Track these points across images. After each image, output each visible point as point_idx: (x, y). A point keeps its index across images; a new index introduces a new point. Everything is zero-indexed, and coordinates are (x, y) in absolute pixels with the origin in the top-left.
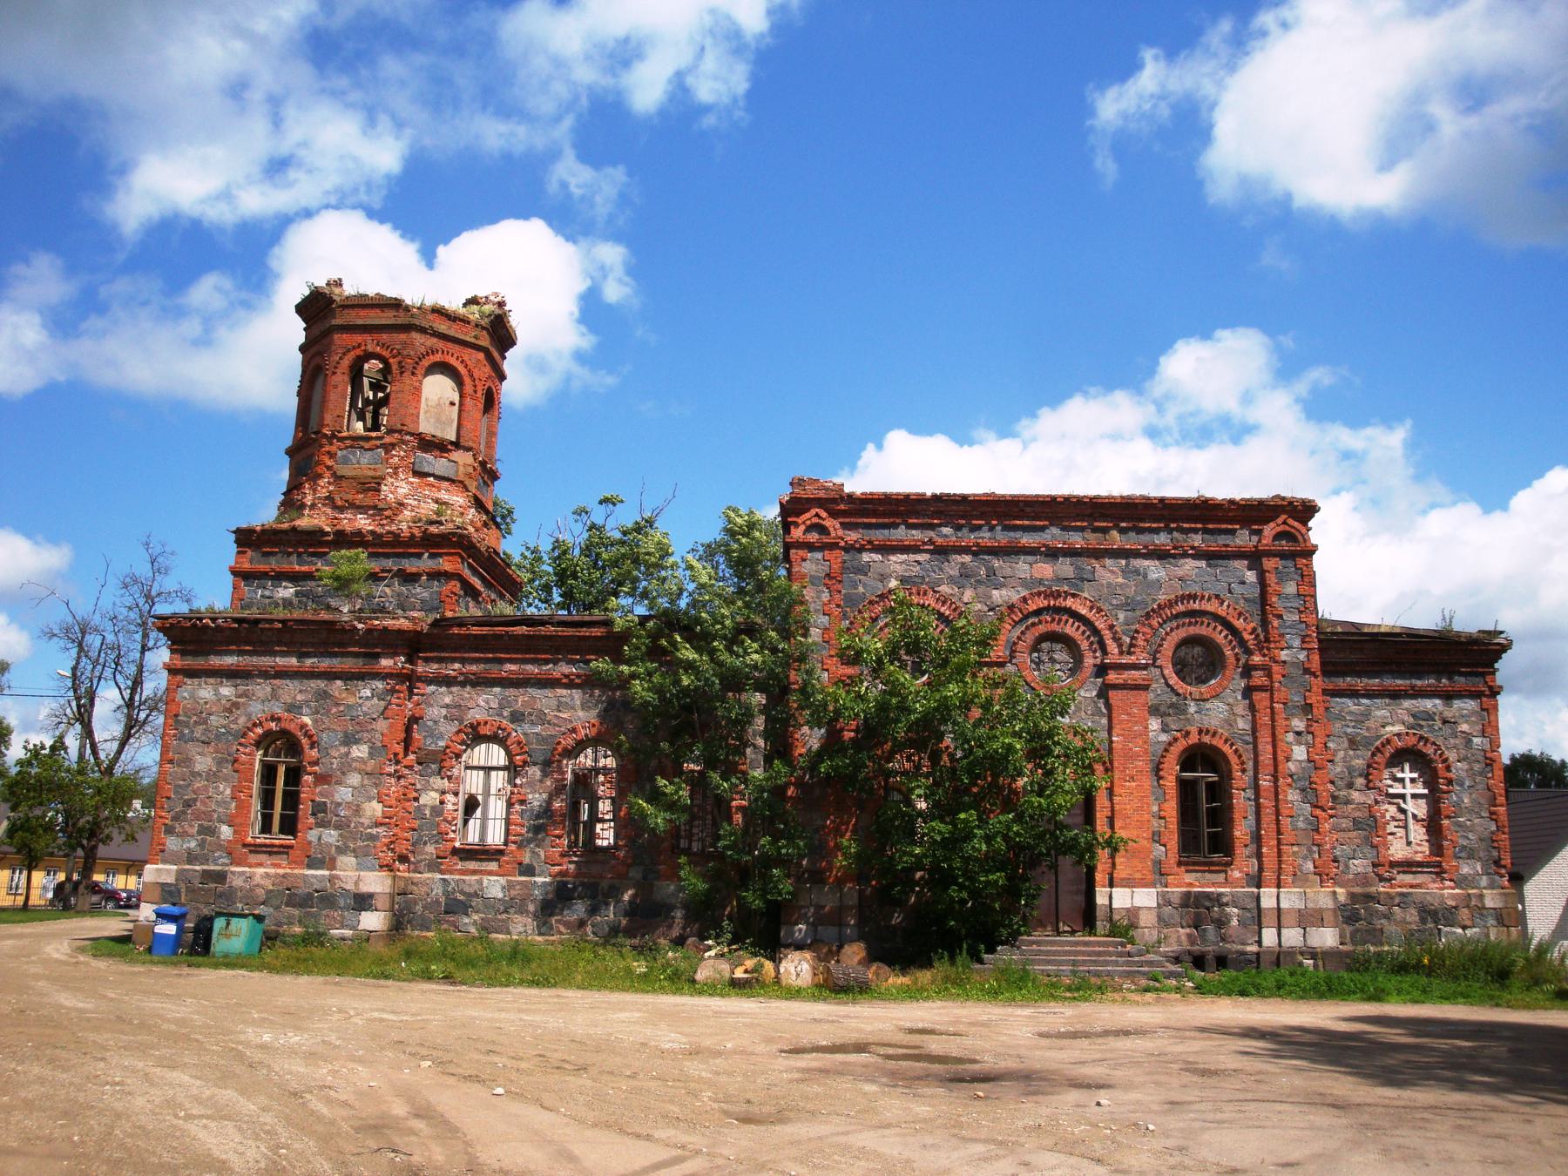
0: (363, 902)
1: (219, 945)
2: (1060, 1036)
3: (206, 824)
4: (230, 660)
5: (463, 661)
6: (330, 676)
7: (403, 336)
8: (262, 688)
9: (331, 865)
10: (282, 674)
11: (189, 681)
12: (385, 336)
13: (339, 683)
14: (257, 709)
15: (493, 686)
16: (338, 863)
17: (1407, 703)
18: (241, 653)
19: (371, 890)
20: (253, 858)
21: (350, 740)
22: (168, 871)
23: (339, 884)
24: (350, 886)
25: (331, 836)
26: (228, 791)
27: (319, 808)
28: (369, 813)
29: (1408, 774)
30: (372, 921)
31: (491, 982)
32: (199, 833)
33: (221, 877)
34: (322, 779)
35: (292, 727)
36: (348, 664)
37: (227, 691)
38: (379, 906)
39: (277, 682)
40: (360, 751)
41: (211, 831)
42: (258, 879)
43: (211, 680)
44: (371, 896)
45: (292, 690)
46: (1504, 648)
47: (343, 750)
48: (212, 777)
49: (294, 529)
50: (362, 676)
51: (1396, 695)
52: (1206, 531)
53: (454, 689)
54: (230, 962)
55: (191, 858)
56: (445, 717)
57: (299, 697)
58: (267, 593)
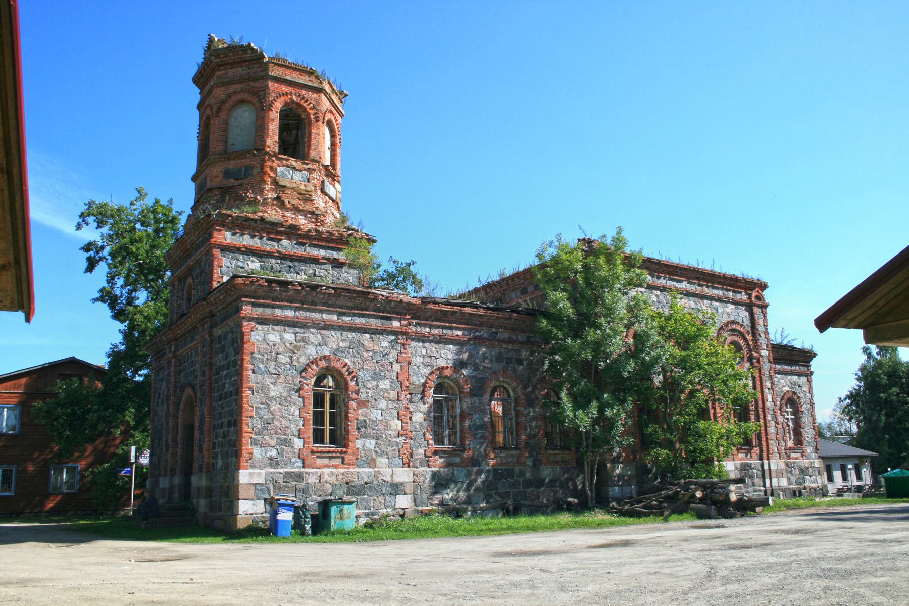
0: (396, 489)
1: (334, 524)
2: (595, 547)
3: (282, 437)
4: (290, 313)
5: (431, 327)
6: (363, 330)
7: (315, 96)
8: (314, 336)
9: (372, 463)
10: (328, 326)
11: (259, 327)
12: (304, 92)
13: (367, 336)
14: (312, 351)
15: (448, 344)
16: (377, 463)
17: (789, 377)
18: (296, 309)
19: (402, 481)
20: (319, 461)
21: (377, 377)
22: (259, 474)
23: (381, 477)
24: (388, 479)
25: (371, 444)
26: (297, 413)
27: (362, 425)
28: (394, 428)
29: (789, 410)
30: (404, 501)
31: (552, 533)
32: (278, 444)
33: (299, 477)
34: (362, 404)
35: (338, 365)
36: (374, 323)
37: (289, 336)
38: (407, 491)
39: (323, 332)
40: (385, 384)
41: (287, 443)
42: (326, 477)
43: (276, 328)
44: (402, 484)
45: (335, 340)
46: (815, 355)
47: (374, 383)
48: (284, 401)
49: (262, 219)
50: (381, 332)
51: (786, 373)
52: (734, 292)
53: (427, 345)
54: (348, 536)
55: (273, 462)
56: (423, 363)
57: (341, 344)
58: (240, 264)
